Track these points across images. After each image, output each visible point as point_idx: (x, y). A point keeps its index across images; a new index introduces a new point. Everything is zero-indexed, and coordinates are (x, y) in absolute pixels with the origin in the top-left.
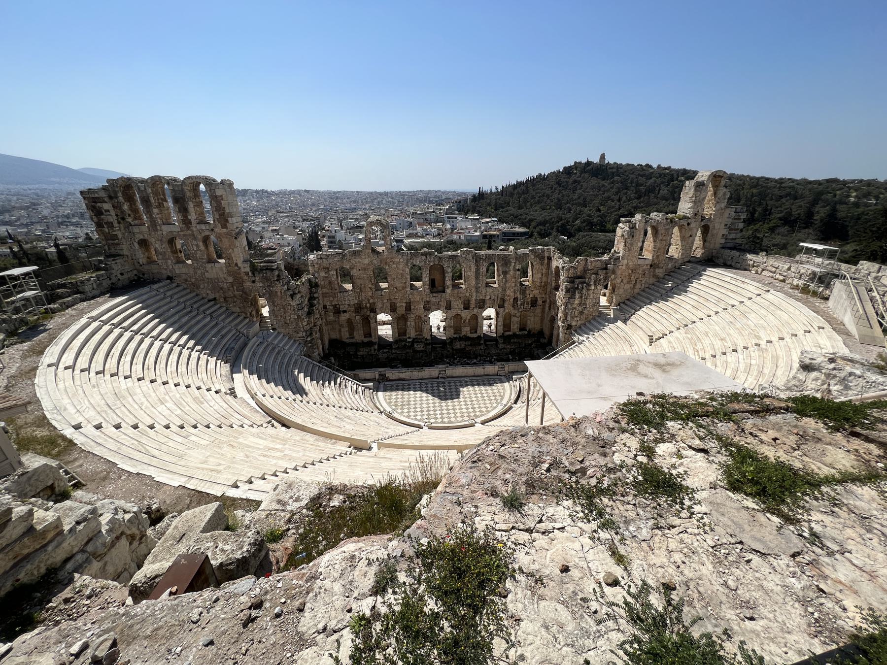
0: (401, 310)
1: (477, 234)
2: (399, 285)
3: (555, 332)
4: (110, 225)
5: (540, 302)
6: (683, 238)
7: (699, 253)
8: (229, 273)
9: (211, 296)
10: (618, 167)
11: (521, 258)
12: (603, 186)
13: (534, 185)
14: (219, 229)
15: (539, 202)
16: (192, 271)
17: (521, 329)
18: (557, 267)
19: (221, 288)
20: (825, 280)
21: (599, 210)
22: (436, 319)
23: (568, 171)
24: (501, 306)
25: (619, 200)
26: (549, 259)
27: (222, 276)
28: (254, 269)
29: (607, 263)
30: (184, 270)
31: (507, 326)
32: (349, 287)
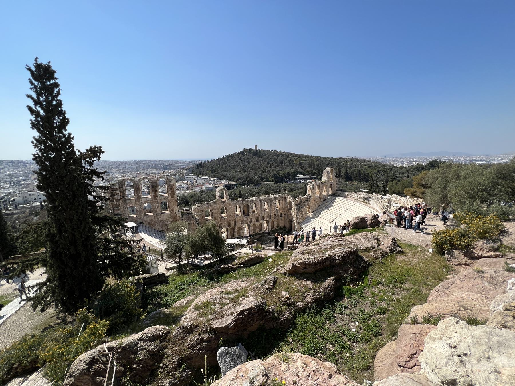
0: (232, 225)
1: (211, 186)
2: (232, 214)
3: (293, 226)
4: (118, 200)
5: (283, 215)
6: (326, 188)
7: (331, 193)
8: (171, 217)
9: (160, 230)
10: (264, 151)
11: (275, 199)
12: (261, 160)
13: (228, 160)
14: (170, 198)
15: (234, 168)
16: (153, 219)
17: (277, 227)
18: (290, 201)
19: (166, 225)
20: (368, 199)
21: (263, 172)
22: (265, 225)
23: (242, 153)
24: (270, 218)
25: (271, 167)
26: (285, 198)
27: (167, 218)
28: (182, 214)
29: (307, 198)
30: (149, 218)
31: (272, 227)
32: (209, 218)
